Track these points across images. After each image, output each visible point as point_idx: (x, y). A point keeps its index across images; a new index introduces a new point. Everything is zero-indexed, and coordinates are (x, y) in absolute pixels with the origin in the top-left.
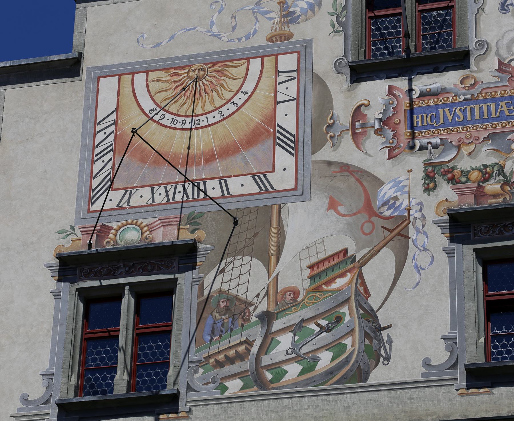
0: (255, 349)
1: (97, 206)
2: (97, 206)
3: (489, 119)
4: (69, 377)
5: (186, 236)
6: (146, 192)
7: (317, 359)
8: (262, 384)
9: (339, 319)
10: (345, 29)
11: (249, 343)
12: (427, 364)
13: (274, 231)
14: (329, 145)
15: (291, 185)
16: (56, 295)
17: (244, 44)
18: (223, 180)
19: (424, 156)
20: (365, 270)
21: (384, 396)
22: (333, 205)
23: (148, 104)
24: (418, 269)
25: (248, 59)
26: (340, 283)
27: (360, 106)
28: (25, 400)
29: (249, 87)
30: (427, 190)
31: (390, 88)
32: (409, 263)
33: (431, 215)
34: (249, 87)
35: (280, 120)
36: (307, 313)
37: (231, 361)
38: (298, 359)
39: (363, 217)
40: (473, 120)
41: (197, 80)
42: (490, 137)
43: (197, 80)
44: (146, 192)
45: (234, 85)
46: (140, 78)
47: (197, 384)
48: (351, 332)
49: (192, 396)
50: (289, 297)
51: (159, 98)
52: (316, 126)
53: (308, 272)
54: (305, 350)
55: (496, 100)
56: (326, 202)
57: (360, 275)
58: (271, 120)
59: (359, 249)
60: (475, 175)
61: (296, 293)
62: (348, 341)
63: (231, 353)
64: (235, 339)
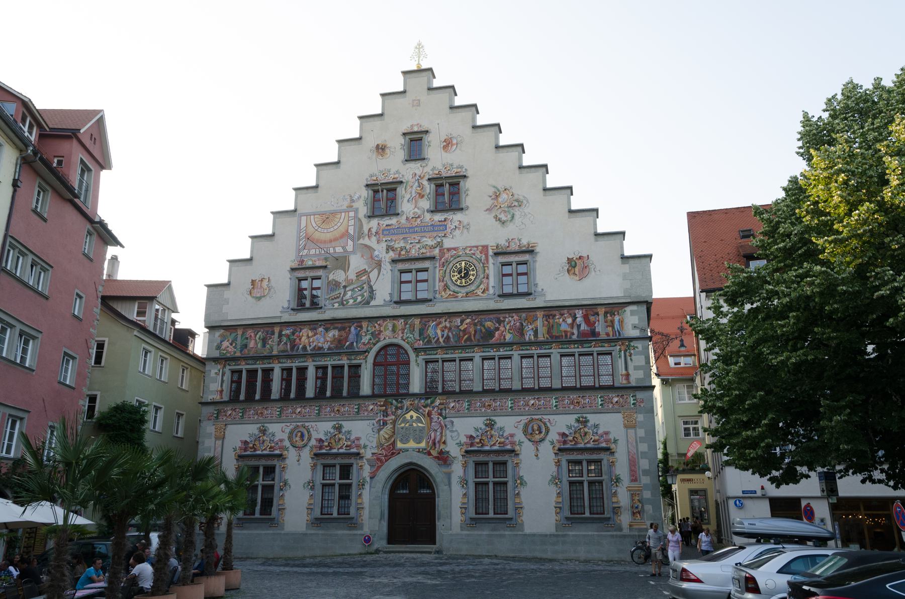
0: (342, 296)
1: (301, 254)
2: (301, 254)
3: (403, 233)
4: (294, 302)
5: (324, 264)
6: (314, 250)
7: (357, 299)
8: (343, 305)
9: (363, 288)
10: (367, 204)
11: (340, 294)
12: (384, 300)
13: (347, 263)
14: (361, 239)
15: (352, 250)
16: (290, 279)
17: (340, 208)
18: (334, 248)
19: (386, 243)
20: (370, 275)
21: (373, 309)
22: (362, 256)
23: (314, 225)
24: (383, 275)
25: (341, 213)
26: (364, 278)
27: (370, 229)
28: (283, 308)
29: (341, 221)
30: (387, 253)
31: (378, 224)
32: (381, 273)
33: (388, 260)
34: (341, 221)
35: (349, 231)
36: (355, 286)
37: (335, 298)
38: (353, 298)
39: (370, 260)
40: (399, 234)
41: (328, 218)
42: (404, 238)
43: (328, 218)
44: (314, 250)
45: (337, 220)
46: (312, 217)
47: (327, 304)
48: (366, 292)
49: (326, 308)
50: (351, 281)
51: (317, 223)
52: (359, 232)
53: (356, 275)
54: (354, 296)
55: (405, 228)
56: (361, 255)
57: (369, 276)
58: (347, 231)
59: (369, 269)
60: (399, 249)
61: (352, 281)
62: (365, 294)
63: (336, 296)
64: (337, 293)
